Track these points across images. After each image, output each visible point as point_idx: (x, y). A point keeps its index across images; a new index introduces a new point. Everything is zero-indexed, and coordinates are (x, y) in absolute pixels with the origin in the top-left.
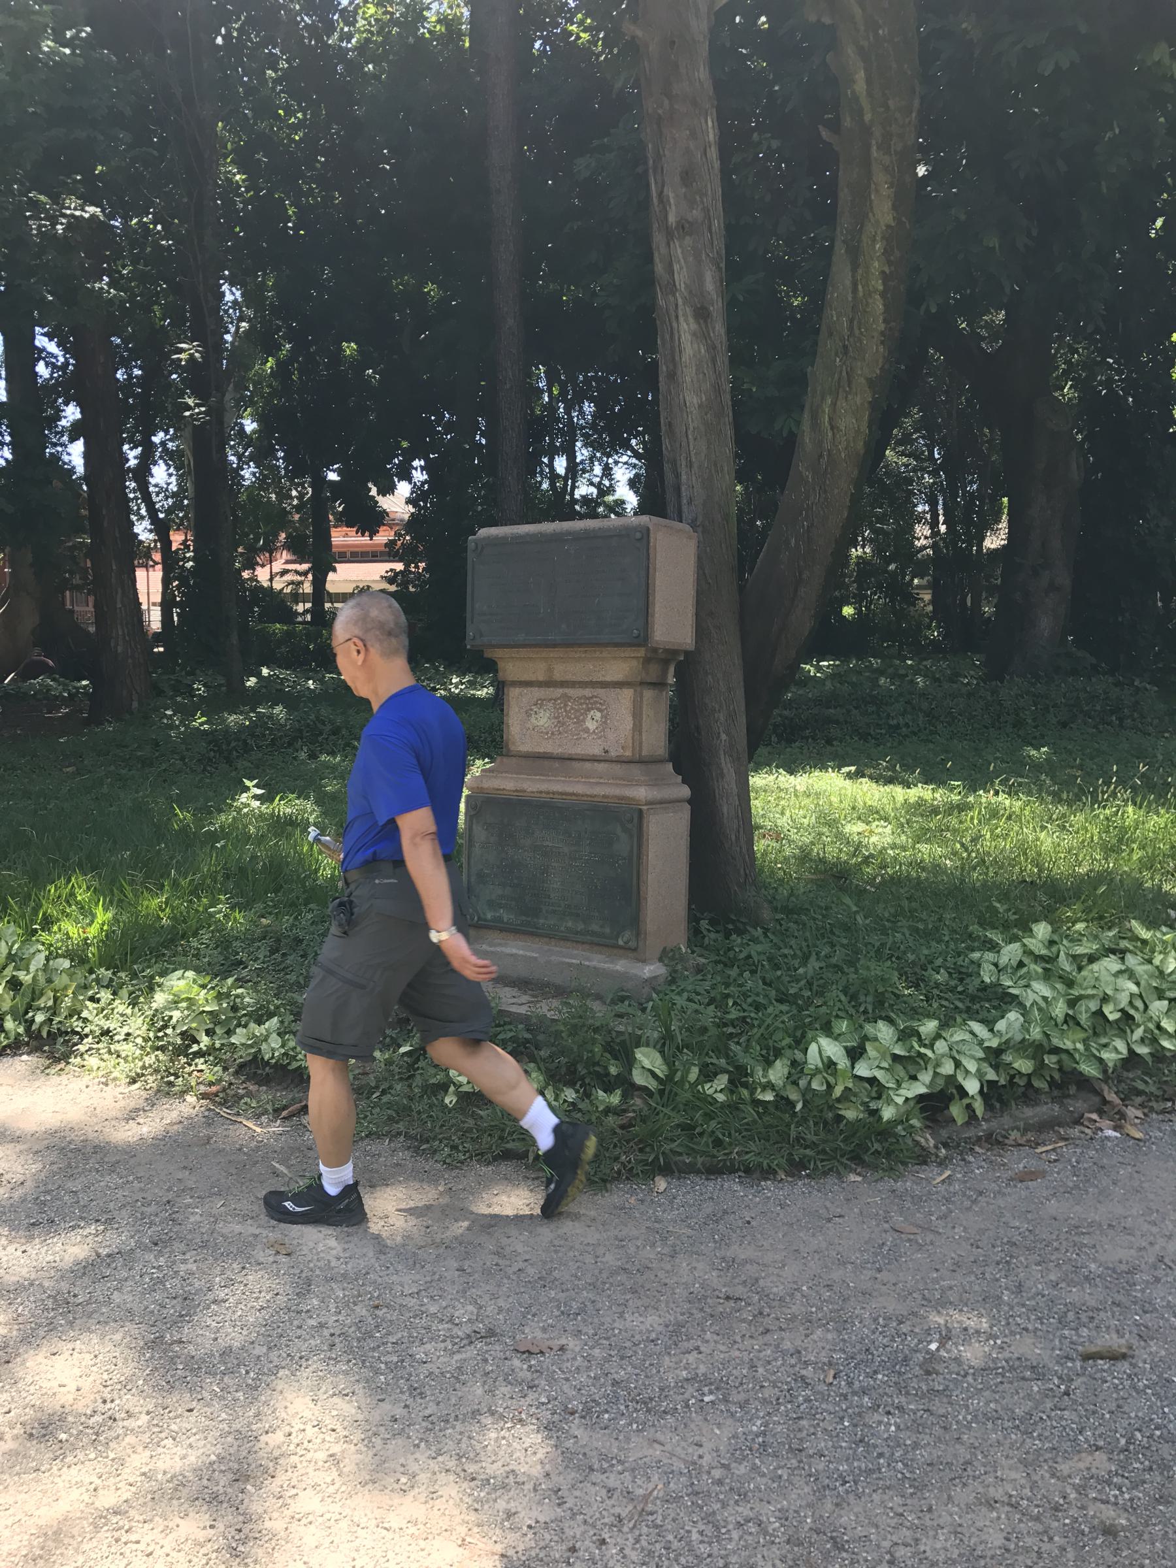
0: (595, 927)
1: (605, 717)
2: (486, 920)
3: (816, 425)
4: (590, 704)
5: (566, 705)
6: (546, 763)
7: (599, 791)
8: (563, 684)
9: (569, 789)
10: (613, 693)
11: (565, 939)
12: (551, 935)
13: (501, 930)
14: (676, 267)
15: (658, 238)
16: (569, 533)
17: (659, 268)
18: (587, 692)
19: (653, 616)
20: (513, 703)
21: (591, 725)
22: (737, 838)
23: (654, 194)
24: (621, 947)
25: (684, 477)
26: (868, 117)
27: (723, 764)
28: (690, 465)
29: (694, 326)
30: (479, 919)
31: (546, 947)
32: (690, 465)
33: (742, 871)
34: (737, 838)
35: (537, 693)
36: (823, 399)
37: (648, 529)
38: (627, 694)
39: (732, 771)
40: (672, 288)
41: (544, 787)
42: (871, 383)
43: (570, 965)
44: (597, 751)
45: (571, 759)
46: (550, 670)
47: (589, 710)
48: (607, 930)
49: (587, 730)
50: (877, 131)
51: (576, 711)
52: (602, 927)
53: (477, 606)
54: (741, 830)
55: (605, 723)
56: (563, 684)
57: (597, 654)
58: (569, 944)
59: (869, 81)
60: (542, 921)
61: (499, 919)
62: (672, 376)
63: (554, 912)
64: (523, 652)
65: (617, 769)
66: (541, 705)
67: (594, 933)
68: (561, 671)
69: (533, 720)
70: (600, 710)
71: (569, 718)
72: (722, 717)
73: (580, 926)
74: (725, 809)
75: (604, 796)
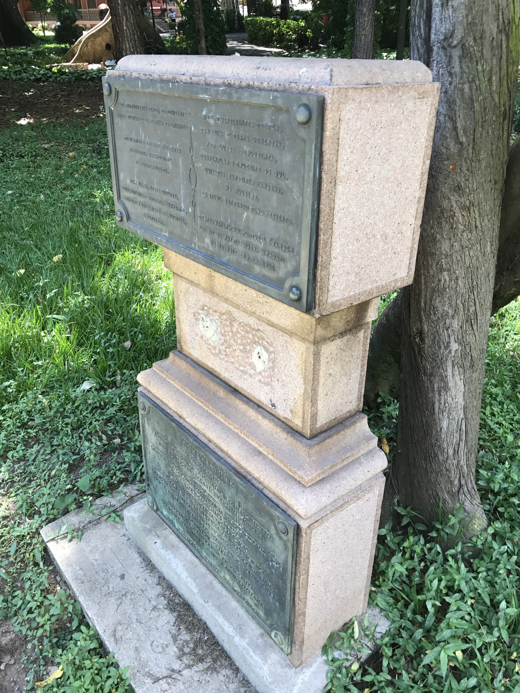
19: (326, 267)
22: (456, 452)
27: (450, 377)
33: (456, 482)
34: (456, 452)
37: (322, 104)
39: (461, 384)
45: (235, 391)
54: (462, 445)
72: (456, 324)
74: (445, 424)
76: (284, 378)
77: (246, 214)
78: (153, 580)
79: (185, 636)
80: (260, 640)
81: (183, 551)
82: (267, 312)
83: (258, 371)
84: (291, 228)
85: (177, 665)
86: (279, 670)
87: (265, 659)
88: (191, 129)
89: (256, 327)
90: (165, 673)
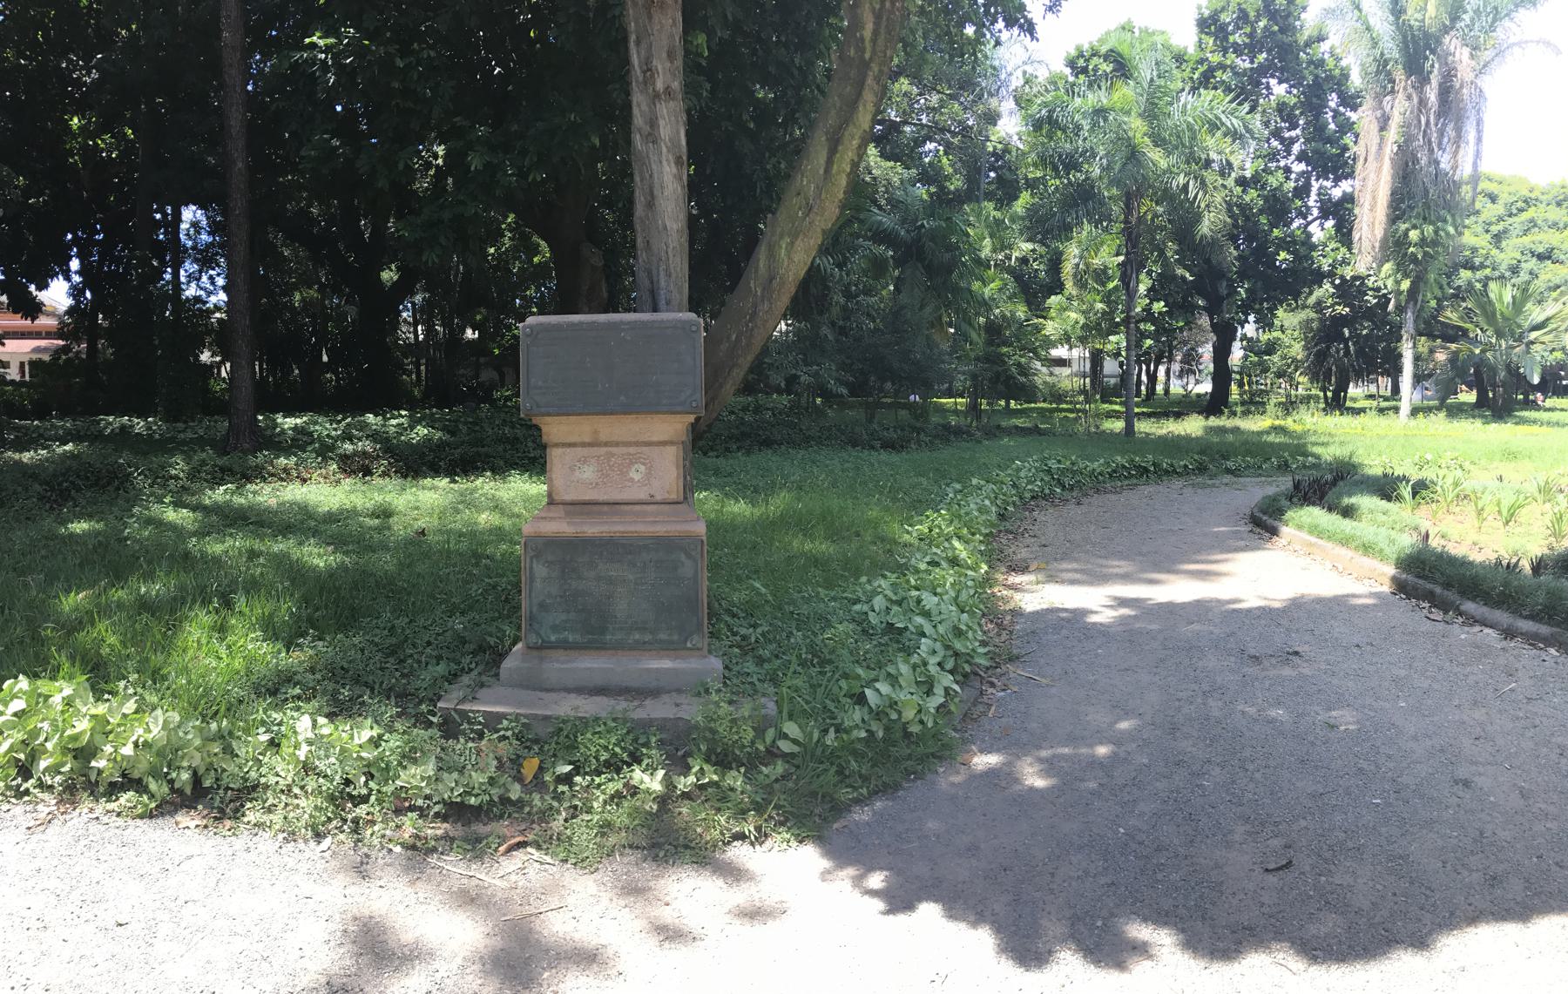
0: (663, 636)
1: (650, 469)
3: (772, 255)
6: (595, 508)
9: (632, 528)
12: (618, 647)
14: (662, 123)
15: (639, 100)
16: (622, 322)
17: (638, 120)
18: (632, 450)
20: (555, 461)
21: (637, 477)
23: (635, 60)
25: (663, 283)
26: (867, 56)
29: (674, 170)
36: (781, 237)
40: (652, 138)
41: (605, 528)
42: (824, 231)
44: (643, 495)
46: (596, 432)
47: (632, 463)
48: (675, 637)
49: (632, 480)
50: (875, 68)
56: (606, 444)
59: (876, 33)
61: (566, 641)
62: (651, 204)
73: (648, 637)
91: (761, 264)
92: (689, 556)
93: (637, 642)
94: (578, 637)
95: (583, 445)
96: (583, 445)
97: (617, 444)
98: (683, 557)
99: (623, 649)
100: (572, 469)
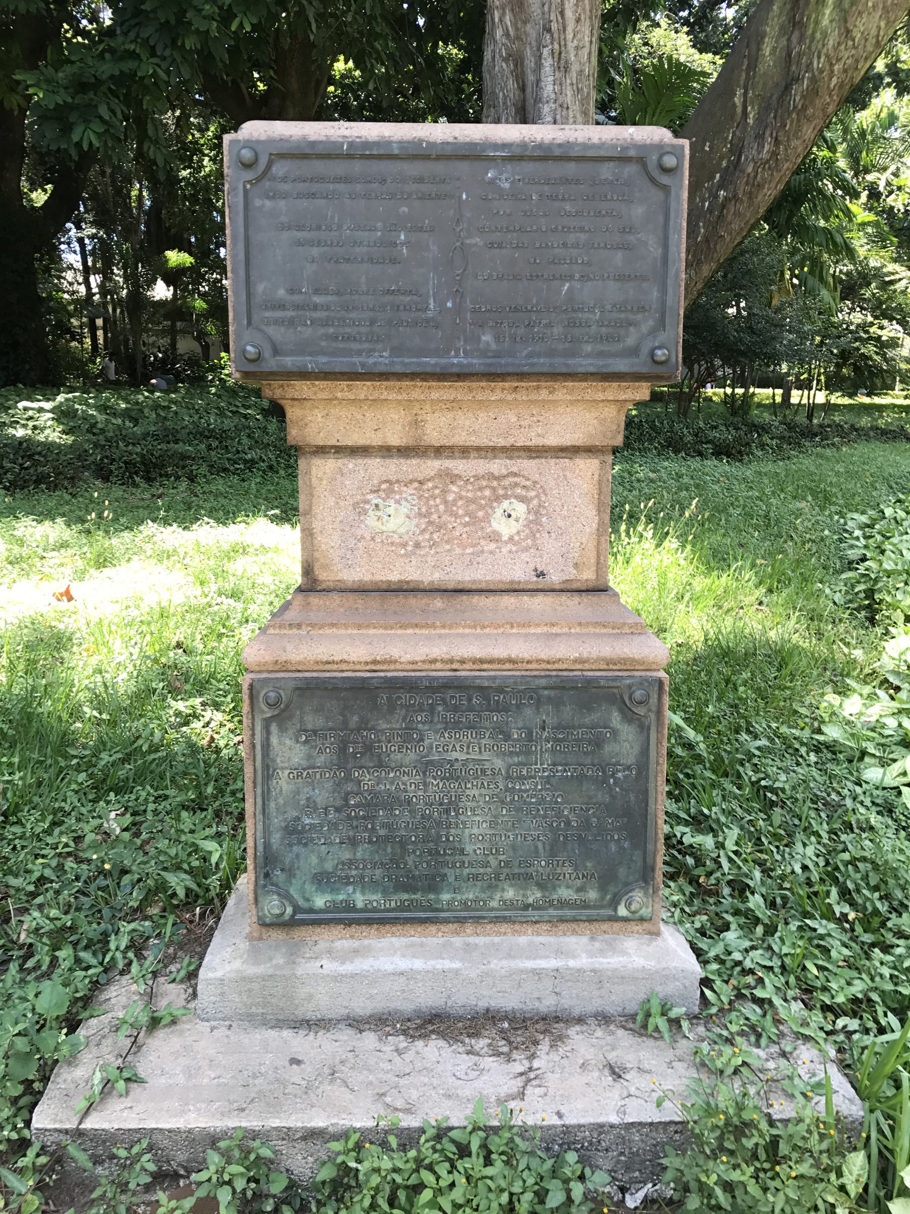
0: (565, 893)
2: (311, 911)
4: (500, 489)
5: (445, 492)
6: (413, 601)
7: (544, 651)
8: (439, 451)
9: (500, 652)
10: (548, 471)
11: (497, 920)
12: (469, 917)
13: (348, 923)
18: (498, 466)
24: (625, 920)
25: (548, 89)
28: (562, 66)
30: (297, 909)
31: (458, 941)
32: (562, 66)
35: (377, 468)
38: (587, 471)
43: (537, 973)
46: (416, 423)
47: (498, 499)
48: (592, 895)
49: (495, 537)
51: (470, 501)
52: (580, 890)
53: (260, 288)
55: (537, 522)
56: (439, 451)
57: (544, 394)
58: (504, 927)
60: (446, 897)
63: (476, 877)
64: (363, 389)
65: (572, 603)
66: (390, 492)
67: (563, 904)
68: (437, 428)
69: (371, 520)
70: (522, 499)
71: (456, 516)
75: (575, 661)
76: (560, 523)
77: (567, 285)
78: (346, 1035)
79: (481, 1044)
80: (597, 944)
81: (379, 945)
82: (539, 435)
83: (505, 538)
84: (645, 285)
85: (519, 1067)
86: (650, 949)
87: (624, 953)
88: (461, 196)
89: (504, 472)
90: (520, 1082)
91: (767, 50)
92: (629, 716)
93: (508, 905)
94: (375, 898)
95: (386, 451)
96: (386, 451)
97: (465, 451)
98: (616, 719)
99: (477, 920)
100: (360, 509)
